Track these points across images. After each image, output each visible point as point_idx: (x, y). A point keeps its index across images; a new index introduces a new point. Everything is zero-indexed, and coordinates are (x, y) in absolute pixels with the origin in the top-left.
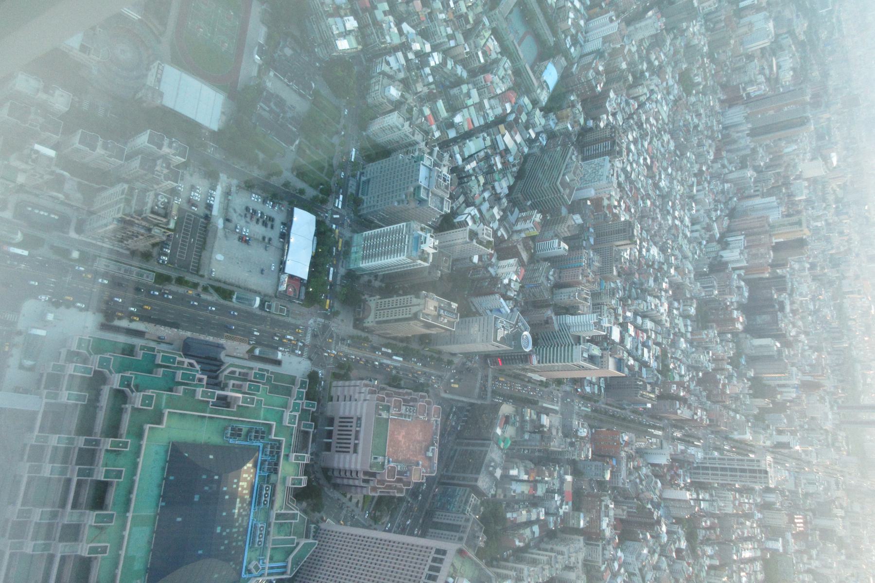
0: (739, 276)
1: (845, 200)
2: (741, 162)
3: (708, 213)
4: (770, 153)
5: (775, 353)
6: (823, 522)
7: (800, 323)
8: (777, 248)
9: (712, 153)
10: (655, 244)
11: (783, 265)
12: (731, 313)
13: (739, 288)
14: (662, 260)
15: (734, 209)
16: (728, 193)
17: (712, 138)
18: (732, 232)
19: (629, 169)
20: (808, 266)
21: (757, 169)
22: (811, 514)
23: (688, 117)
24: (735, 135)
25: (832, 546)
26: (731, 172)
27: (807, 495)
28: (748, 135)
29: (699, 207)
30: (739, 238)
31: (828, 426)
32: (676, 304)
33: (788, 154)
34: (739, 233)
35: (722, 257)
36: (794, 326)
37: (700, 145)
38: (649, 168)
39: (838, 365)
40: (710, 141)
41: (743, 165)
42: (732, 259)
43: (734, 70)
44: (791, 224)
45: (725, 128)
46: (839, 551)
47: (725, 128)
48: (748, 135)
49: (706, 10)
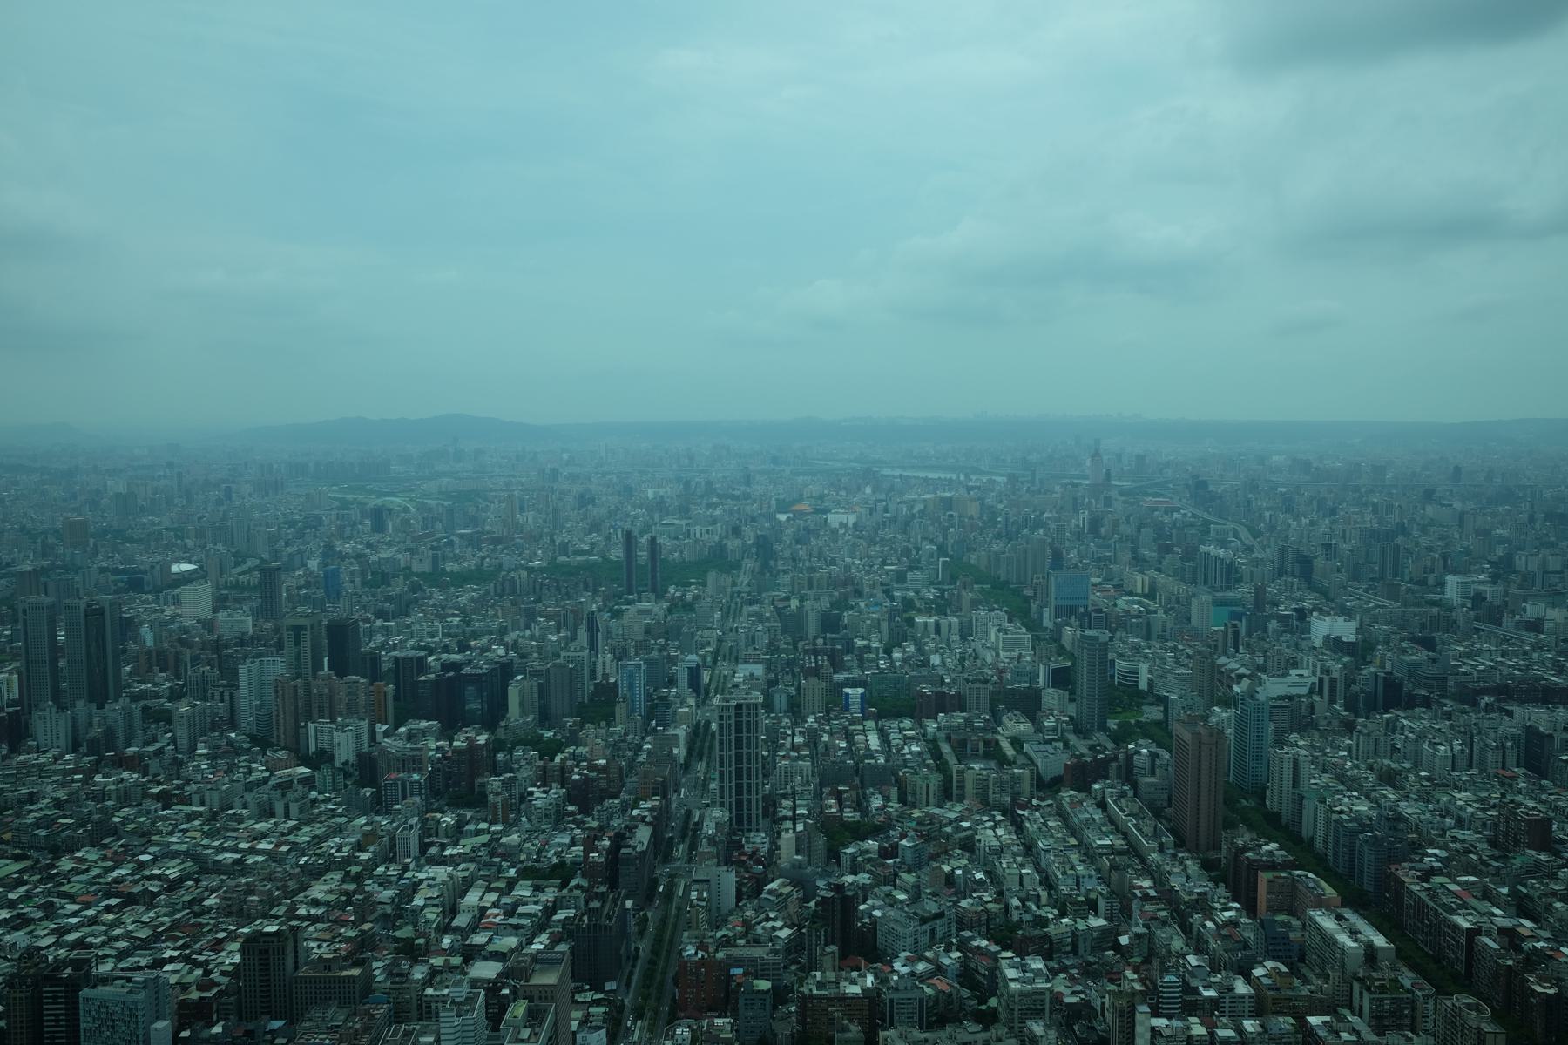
0: (386, 734)
1: (266, 556)
2: (157, 721)
3: (250, 787)
4: (150, 670)
5: (535, 682)
6: (812, 628)
7: (484, 640)
8: (340, 668)
9: (125, 775)
10: (304, 888)
11: (375, 660)
12: (457, 751)
13: (410, 737)
14: (338, 876)
15: (254, 739)
16: (218, 747)
17: (89, 774)
18: (298, 743)
19: (122, 945)
20: (379, 623)
21: (175, 696)
22: (801, 644)
23: (31, 819)
24: (96, 731)
25: (847, 616)
26: (174, 741)
27: (773, 648)
28: (100, 707)
29: (237, 802)
30: (312, 732)
32: (433, 850)
34: (302, 731)
35: (346, 763)
36: (489, 650)
37: (102, 796)
38: (130, 900)
39: (558, 589)
41: (166, 718)
42: (352, 746)
44: (297, 643)
45: (75, 749)
46: (852, 608)
48: (100, 707)
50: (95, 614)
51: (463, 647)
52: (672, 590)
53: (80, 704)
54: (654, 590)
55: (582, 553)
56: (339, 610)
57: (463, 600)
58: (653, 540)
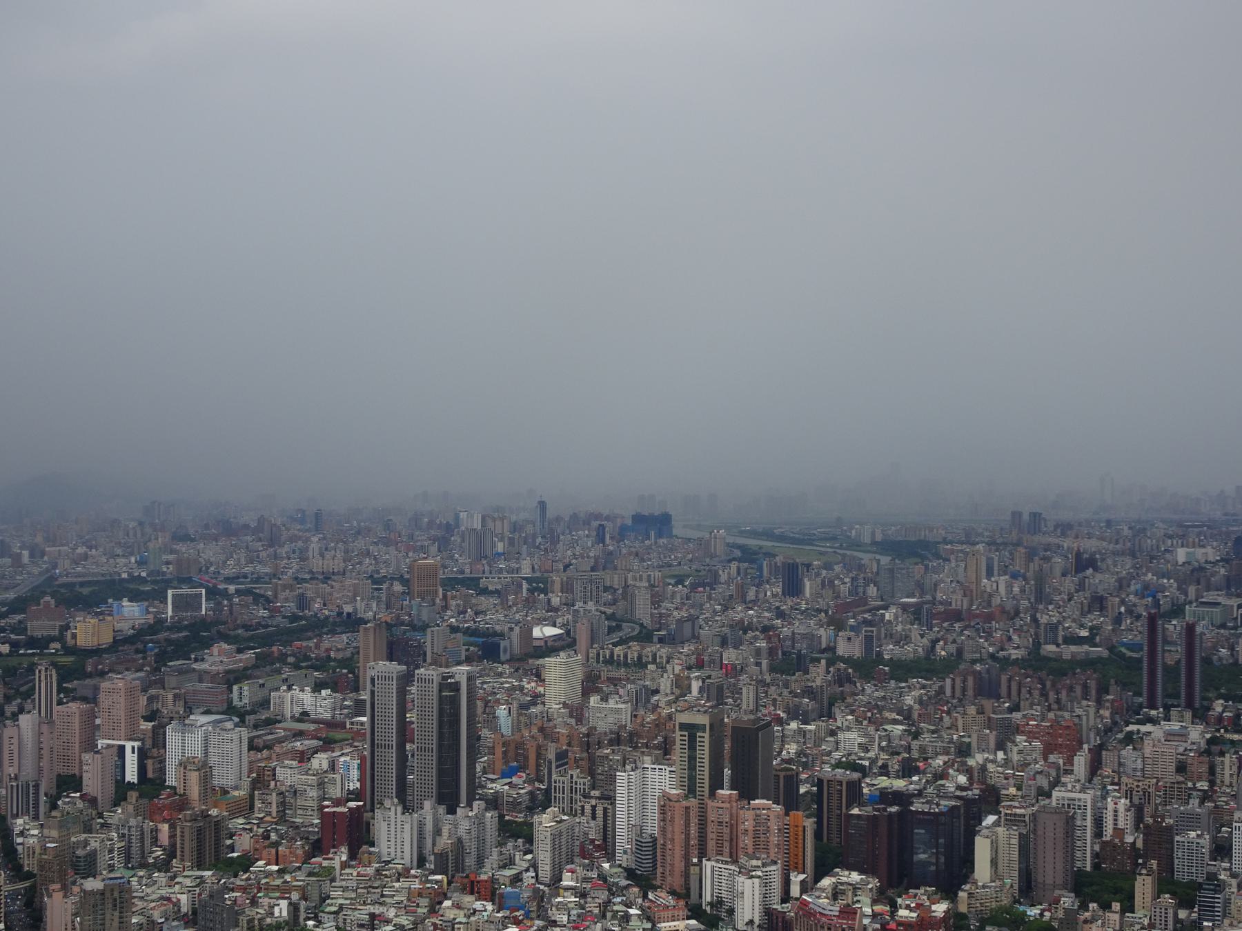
1: (647, 621)
2: (516, 836)
9: (478, 905)
15: (630, 873)
16: (585, 880)
24: (445, 841)
26: (534, 865)
31: (1197, 734)
33: (517, 728)
36: (943, 775)
39: (1044, 694)
40: (447, 903)
43: (282, 818)
47: (421, 862)
48: (451, 811)
49: (117, 860)
50: (449, 688)
51: (908, 770)
52: (1218, 706)
53: (427, 805)
54: (1189, 705)
55: (1079, 641)
56: (745, 706)
57: (909, 700)
58: (1190, 629)
